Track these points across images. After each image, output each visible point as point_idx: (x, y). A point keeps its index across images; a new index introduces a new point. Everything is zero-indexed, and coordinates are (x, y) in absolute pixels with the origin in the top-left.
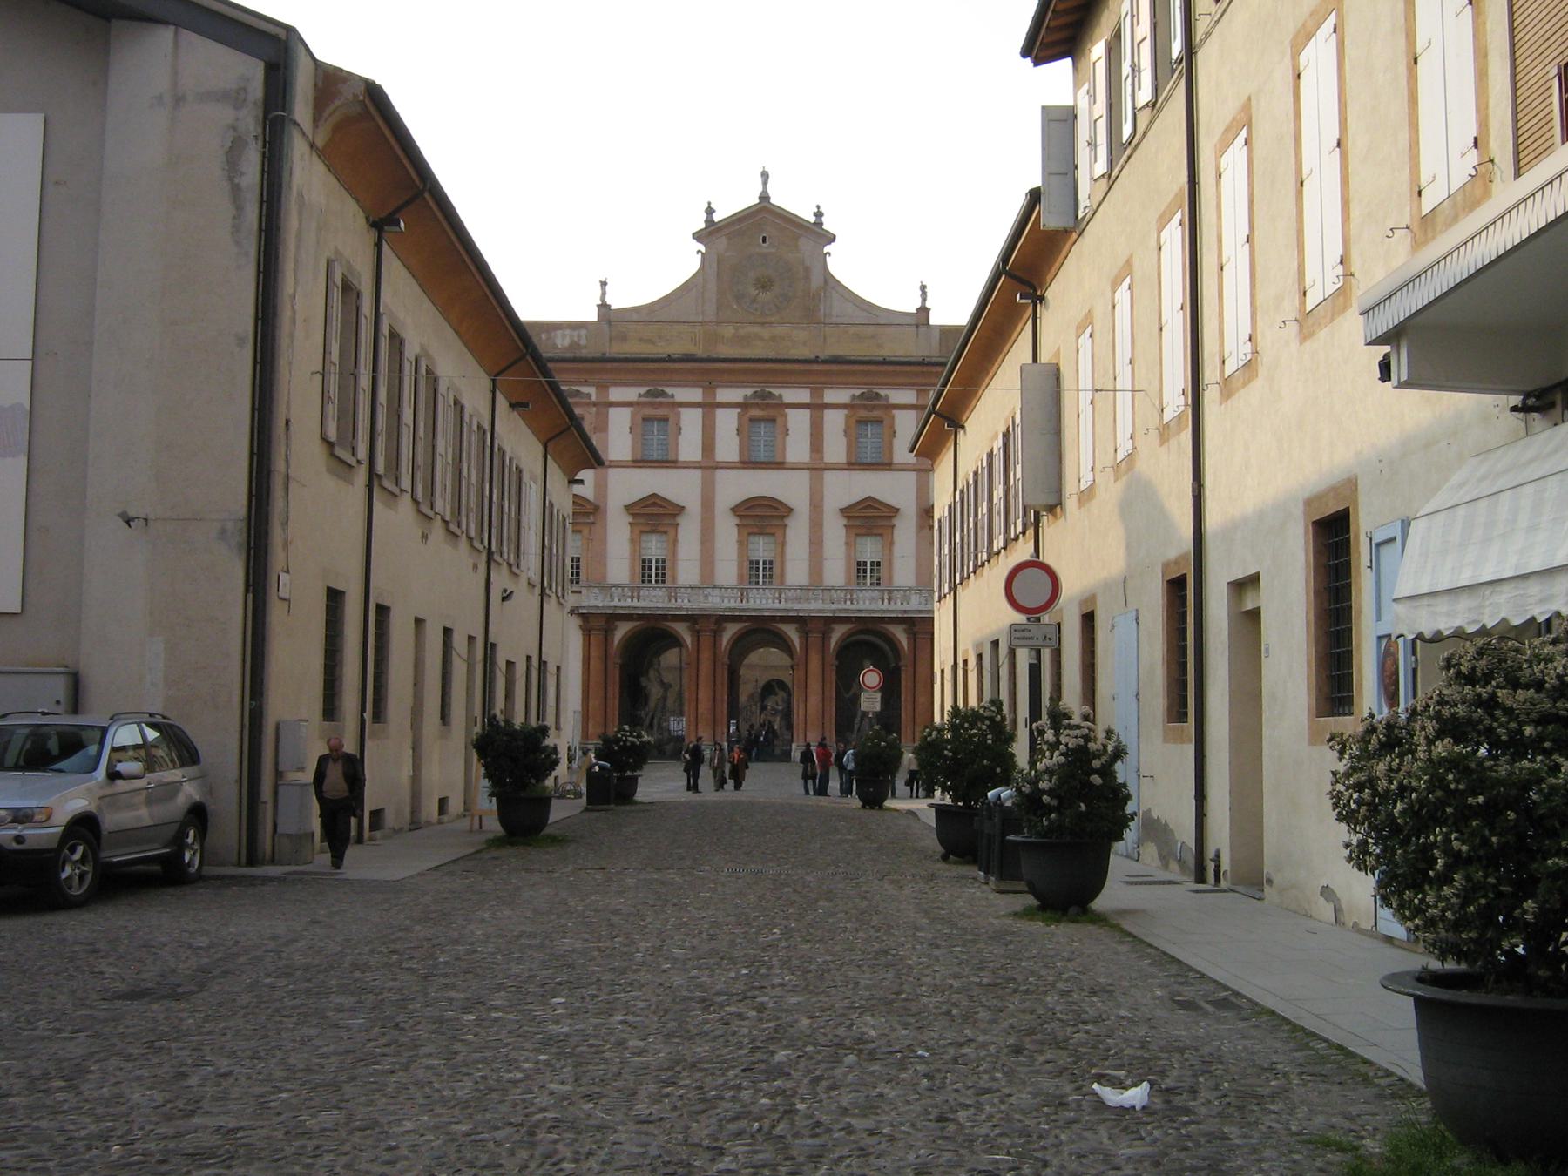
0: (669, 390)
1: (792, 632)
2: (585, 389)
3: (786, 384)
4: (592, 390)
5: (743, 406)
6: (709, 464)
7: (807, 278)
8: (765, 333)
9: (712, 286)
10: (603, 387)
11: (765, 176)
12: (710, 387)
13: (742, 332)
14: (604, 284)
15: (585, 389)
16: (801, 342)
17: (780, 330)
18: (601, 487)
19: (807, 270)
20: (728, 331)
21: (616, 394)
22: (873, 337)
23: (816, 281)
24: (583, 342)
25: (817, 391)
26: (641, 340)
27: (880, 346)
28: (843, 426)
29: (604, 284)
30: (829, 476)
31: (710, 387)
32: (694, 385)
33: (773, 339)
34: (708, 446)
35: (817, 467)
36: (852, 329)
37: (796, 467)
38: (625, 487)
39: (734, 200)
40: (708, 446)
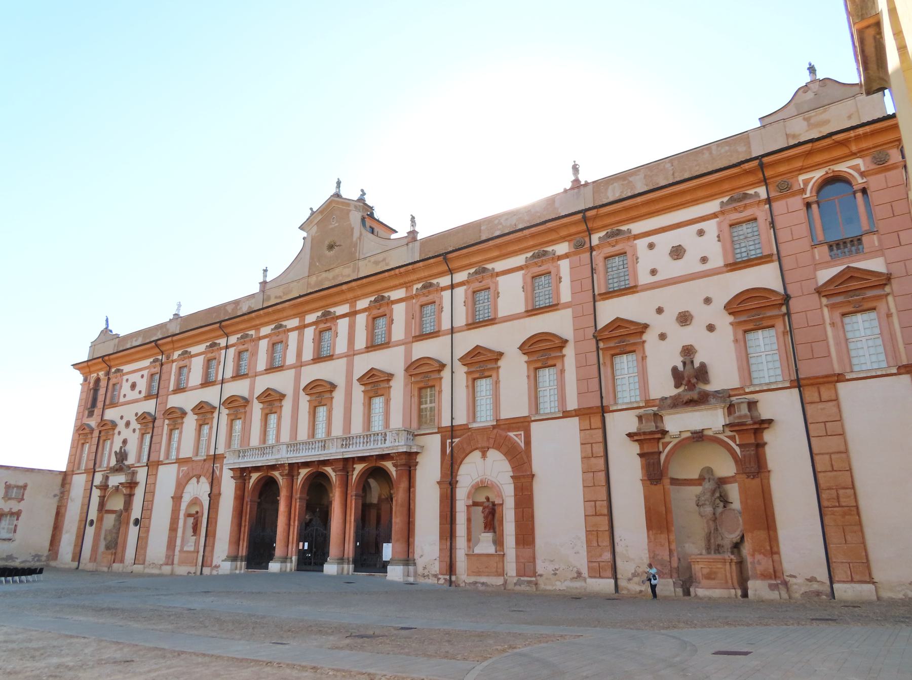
2: (250, 333)
3: (336, 304)
4: (252, 332)
7: (352, 234)
8: (330, 275)
9: (308, 257)
10: (257, 328)
11: (339, 183)
13: (320, 278)
14: (265, 271)
15: (250, 333)
17: (337, 271)
18: (252, 389)
19: (353, 229)
22: (384, 260)
26: (276, 297)
28: (365, 324)
31: (302, 315)
32: (294, 316)
33: (334, 278)
35: (351, 354)
36: (373, 259)
37: (340, 357)
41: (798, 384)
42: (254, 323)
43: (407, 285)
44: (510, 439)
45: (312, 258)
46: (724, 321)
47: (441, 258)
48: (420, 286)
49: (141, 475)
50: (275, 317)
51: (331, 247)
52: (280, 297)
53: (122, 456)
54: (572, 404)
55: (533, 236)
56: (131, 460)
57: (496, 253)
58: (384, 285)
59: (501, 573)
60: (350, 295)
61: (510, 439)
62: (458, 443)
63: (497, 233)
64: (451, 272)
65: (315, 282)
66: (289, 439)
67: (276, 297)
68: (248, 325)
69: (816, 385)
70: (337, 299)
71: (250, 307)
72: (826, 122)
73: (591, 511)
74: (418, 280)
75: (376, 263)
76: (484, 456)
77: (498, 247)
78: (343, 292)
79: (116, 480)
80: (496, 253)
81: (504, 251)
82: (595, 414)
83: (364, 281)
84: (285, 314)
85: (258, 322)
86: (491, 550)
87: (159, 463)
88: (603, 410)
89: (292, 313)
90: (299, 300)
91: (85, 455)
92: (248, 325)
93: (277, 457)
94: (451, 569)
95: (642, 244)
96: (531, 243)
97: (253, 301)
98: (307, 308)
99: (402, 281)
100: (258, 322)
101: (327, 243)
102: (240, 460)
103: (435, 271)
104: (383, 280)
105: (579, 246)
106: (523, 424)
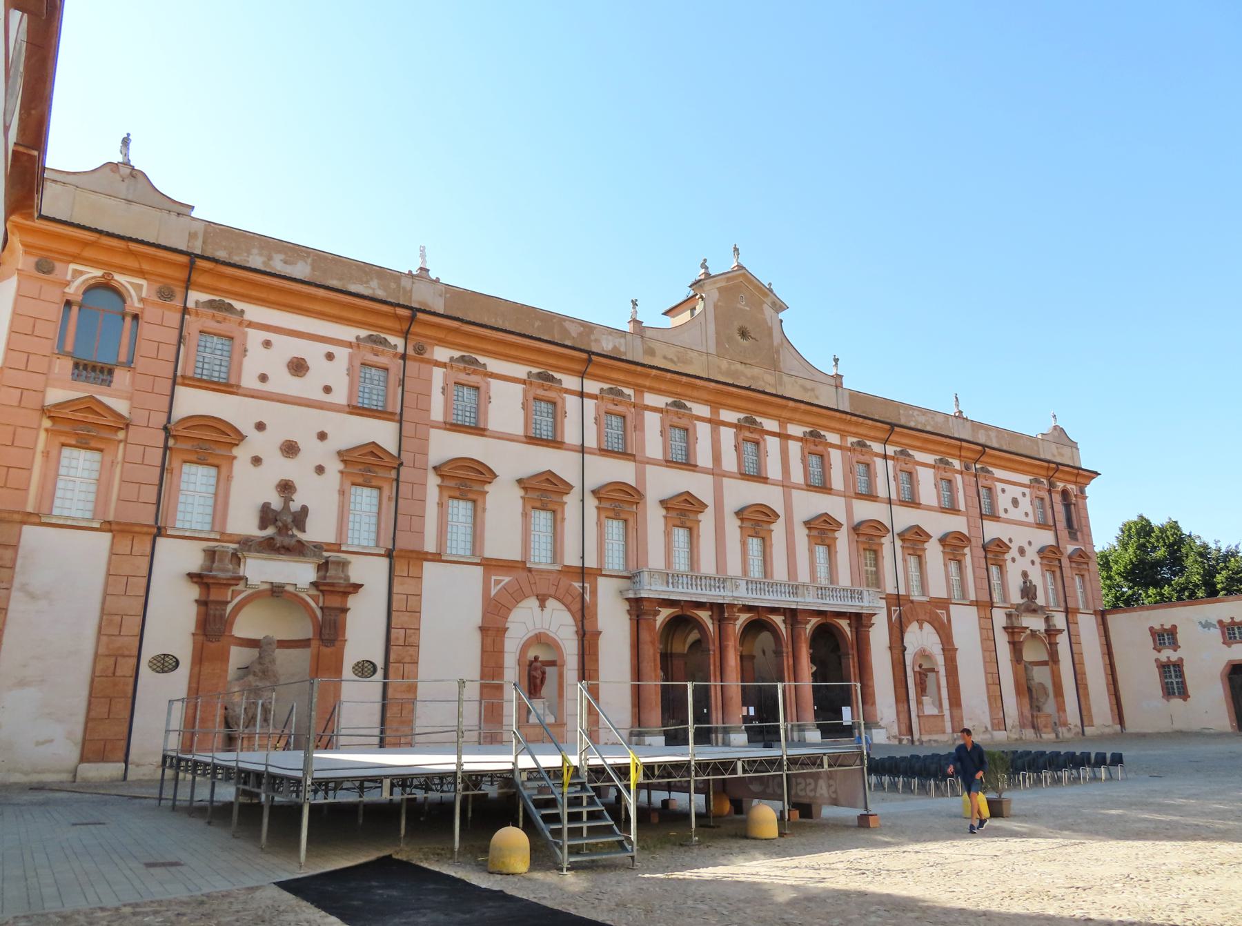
0: (688, 404)
1: (778, 620)
2: (627, 391)
5: (737, 426)
6: (717, 472)
7: (770, 335)
8: (749, 371)
10: (640, 389)
12: (715, 406)
13: (733, 367)
15: (627, 391)
16: (767, 381)
17: (756, 371)
19: (770, 329)
20: (724, 364)
21: (651, 399)
22: (813, 390)
23: (777, 339)
24: (623, 349)
25: (783, 422)
26: (665, 358)
27: (817, 398)
29: (635, 303)
30: (795, 493)
32: (706, 402)
33: (753, 378)
34: (717, 458)
36: (800, 381)
38: (664, 483)
39: (722, 265)
40: (717, 458)
41: (389, 554)
42: (640, 381)
43: (843, 434)
44: (936, 614)
45: (717, 333)
46: (1038, 560)
47: (888, 427)
48: (855, 440)
49: (370, 573)
50: (679, 390)
51: (744, 334)
52: (672, 360)
53: (1028, 591)
54: (972, 597)
55: (948, 445)
56: (1040, 601)
57: (918, 444)
58: (824, 422)
59: (944, 732)
60: (786, 414)
61: (936, 614)
62: (903, 612)
63: (912, 424)
64: (885, 442)
65: (722, 368)
66: (722, 568)
67: (665, 358)
68: (629, 379)
69: (403, 558)
70: (771, 411)
71: (615, 348)
72: (1062, 455)
73: (990, 681)
74: (855, 434)
75: (805, 389)
76: (921, 628)
77: (926, 440)
78: (785, 407)
79: (1035, 623)
80: (918, 444)
81: (925, 446)
82: (985, 606)
83: (814, 409)
84: (695, 394)
85: (647, 383)
86: (935, 711)
87: (1077, 611)
88: (992, 605)
89: (706, 396)
90: (731, 389)
91: (1079, 590)
92: (629, 379)
93: (735, 594)
94: (910, 730)
95: (999, 486)
96: (942, 449)
97: (622, 341)
98: (729, 401)
99: (842, 427)
100: (647, 383)
101: (737, 324)
102: (671, 588)
103: (872, 434)
104: (819, 415)
105: (967, 468)
106: (944, 604)
